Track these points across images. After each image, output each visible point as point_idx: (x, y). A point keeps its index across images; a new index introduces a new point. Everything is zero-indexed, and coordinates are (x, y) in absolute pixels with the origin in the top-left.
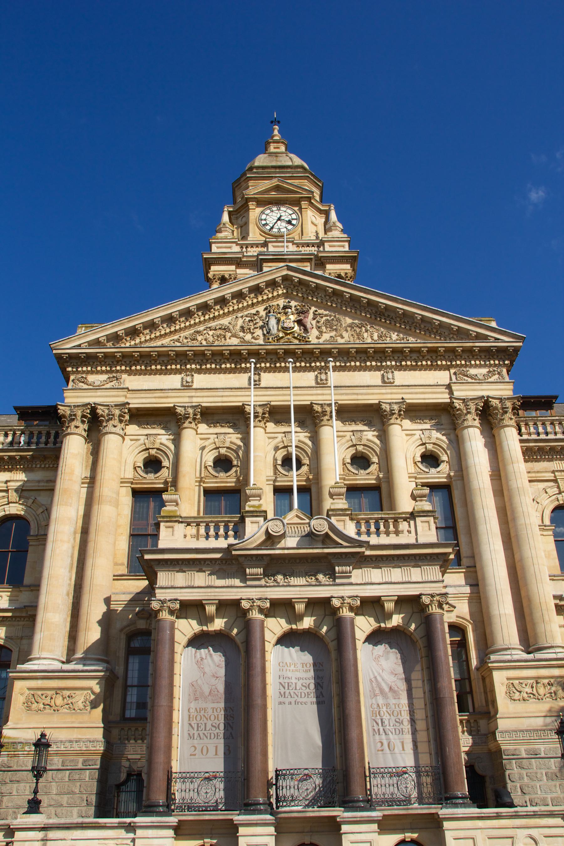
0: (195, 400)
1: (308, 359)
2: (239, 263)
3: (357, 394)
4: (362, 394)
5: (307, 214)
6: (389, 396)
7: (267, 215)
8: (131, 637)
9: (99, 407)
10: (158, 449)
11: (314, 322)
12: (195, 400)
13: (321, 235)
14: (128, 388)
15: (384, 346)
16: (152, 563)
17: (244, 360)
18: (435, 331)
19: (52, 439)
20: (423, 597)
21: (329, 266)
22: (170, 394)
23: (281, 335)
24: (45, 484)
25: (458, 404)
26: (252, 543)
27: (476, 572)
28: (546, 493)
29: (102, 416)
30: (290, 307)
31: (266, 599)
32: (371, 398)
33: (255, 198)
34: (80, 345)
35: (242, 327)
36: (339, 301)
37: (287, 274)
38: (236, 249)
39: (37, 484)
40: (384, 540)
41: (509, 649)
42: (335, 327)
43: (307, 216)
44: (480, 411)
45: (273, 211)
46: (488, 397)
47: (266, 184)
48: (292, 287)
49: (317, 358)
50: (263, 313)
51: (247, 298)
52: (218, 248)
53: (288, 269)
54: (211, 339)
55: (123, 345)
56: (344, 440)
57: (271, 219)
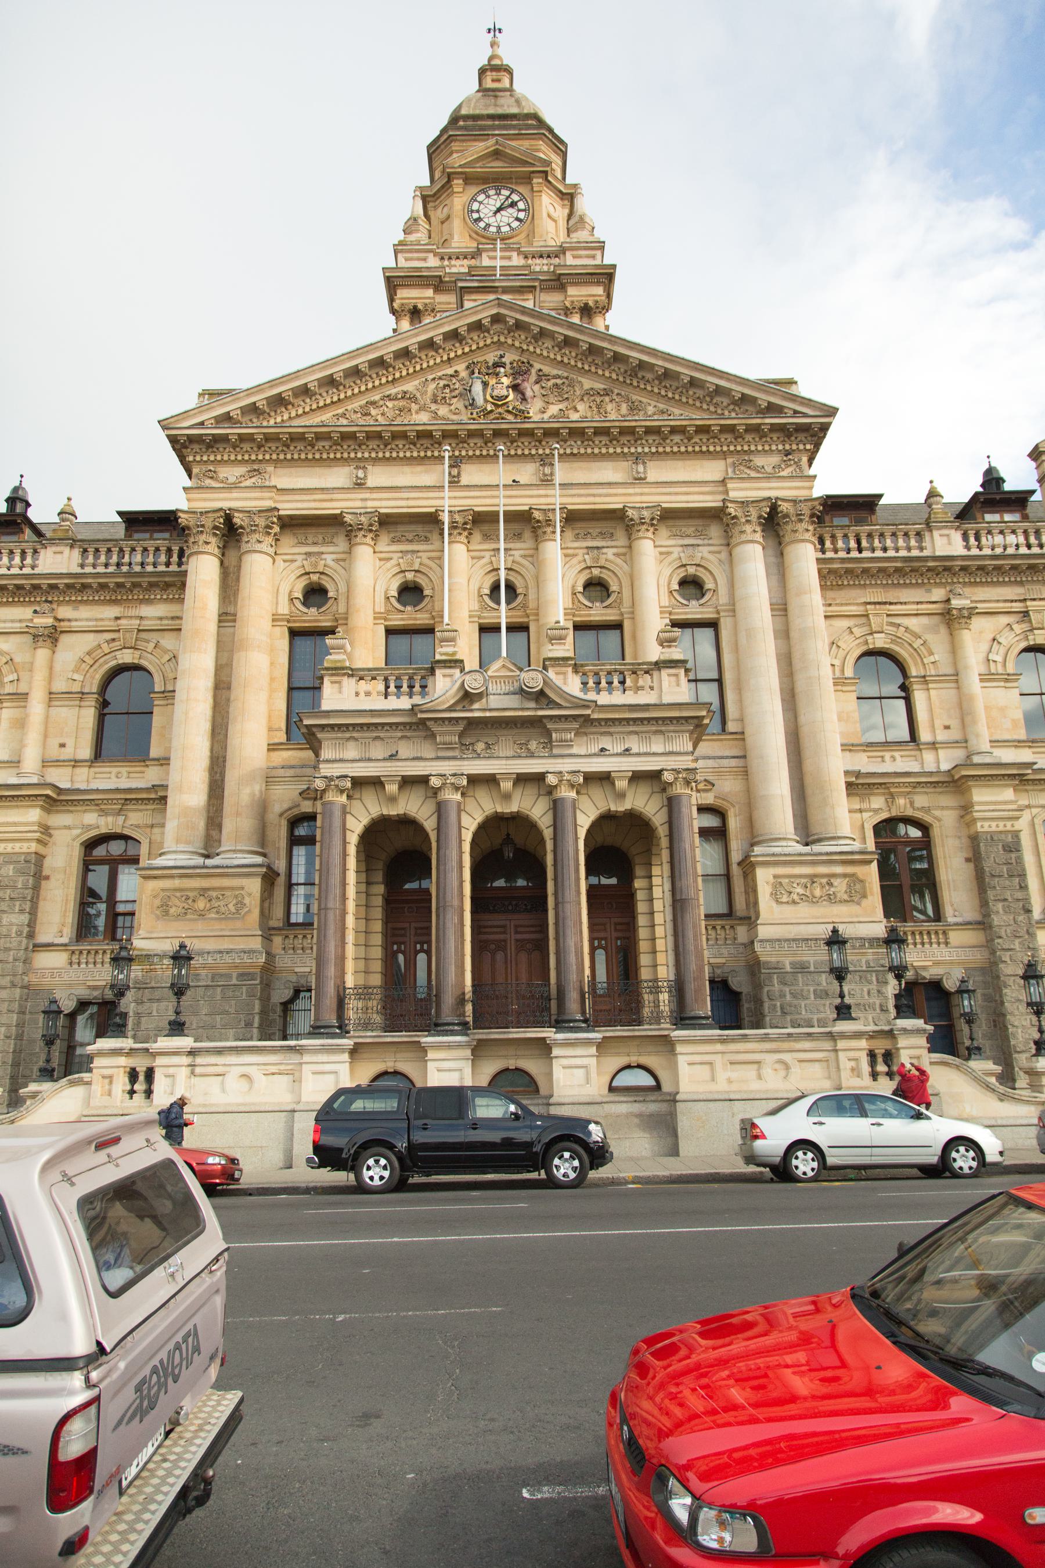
0: (370, 504)
1: (526, 444)
2: (439, 284)
3: (594, 495)
4: (600, 495)
5: (540, 200)
6: (638, 499)
7: (481, 203)
8: (294, 822)
9: (236, 514)
10: (322, 573)
11: (536, 387)
12: (370, 504)
13: (562, 237)
15: (633, 424)
16: (314, 730)
17: (436, 446)
19: (175, 558)
20: (665, 773)
21: (572, 291)
23: (489, 408)
24: (170, 622)
25: (732, 510)
26: (443, 703)
27: (744, 740)
28: (852, 632)
29: (242, 527)
30: (503, 365)
31: (462, 775)
32: (613, 502)
33: (461, 173)
34: (202, 423)
35: (435, 395)
36: (574, 354)
37: (498, 313)
38: (433, 262)
39: (159, 622)
40: (618, 698)
41: (784, 839)
42: (566, 396)
43: (541, 205)
44: (765, 519)
45: (488, 197)
46: (777, 499)
47: (480, 148)
48: (506, 332)
49: (540, 442)
50: (464, 374)
51: (441, 351)
52: (406, 260)
53: (499, 305)
54: (390, 414)
55: (265, 424)
56: (575, 560)
57: (486, 211)
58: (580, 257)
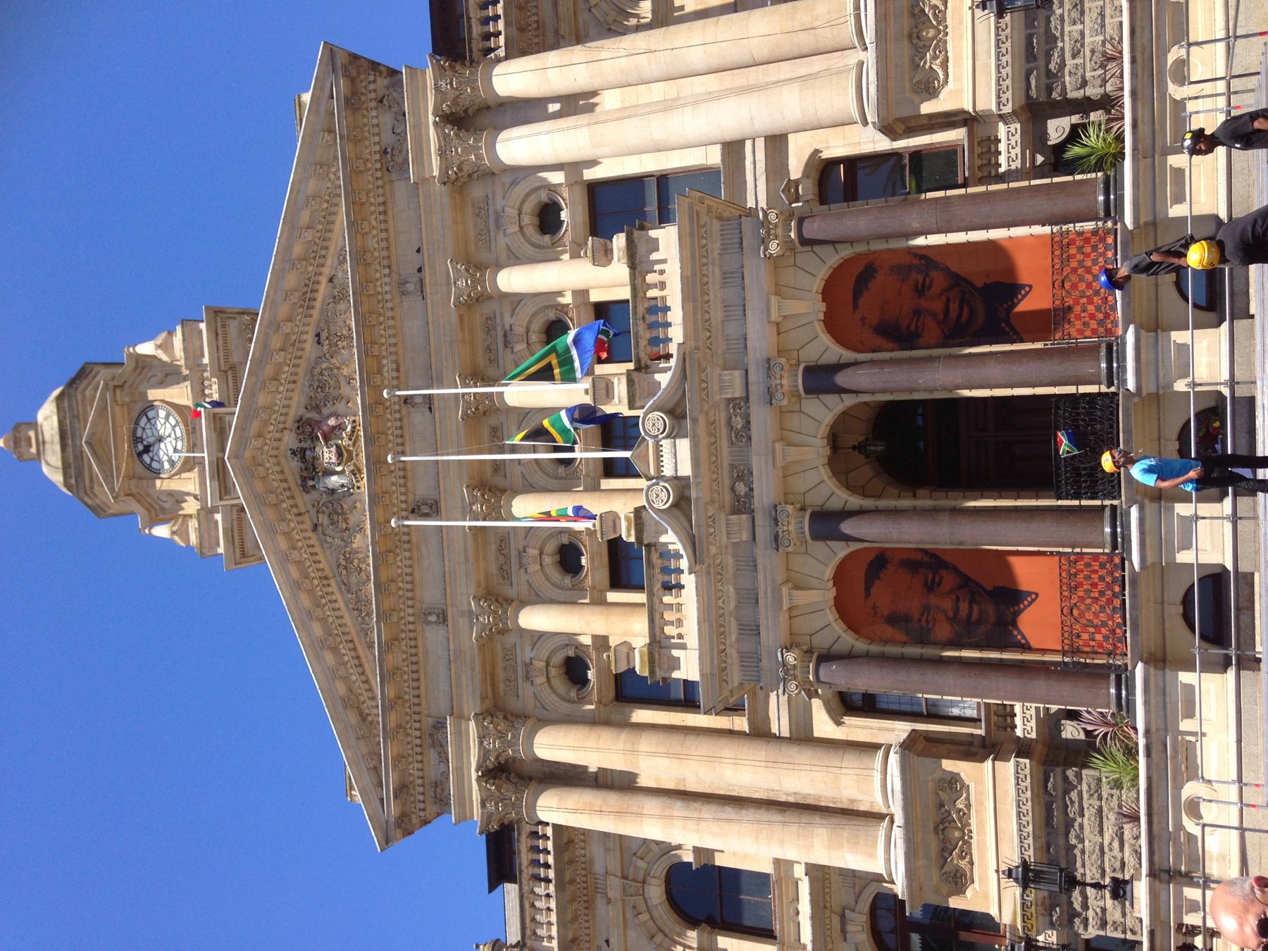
10: (548, 665)
11: (325, 411)
18: (325, 205)
40: (676, 316)
48: (266, 448)
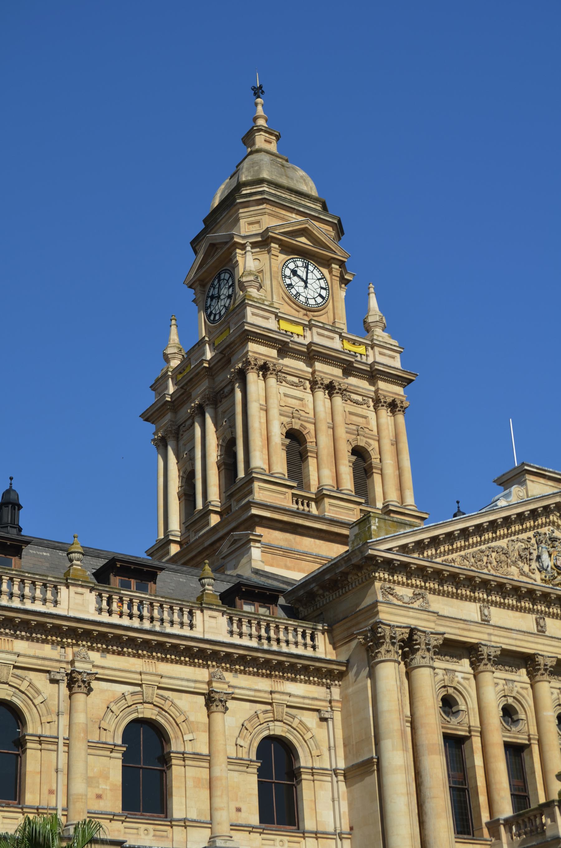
0: (493, 638)
14: (437, 613)
22: (472, 628)
58: (384, 354)
